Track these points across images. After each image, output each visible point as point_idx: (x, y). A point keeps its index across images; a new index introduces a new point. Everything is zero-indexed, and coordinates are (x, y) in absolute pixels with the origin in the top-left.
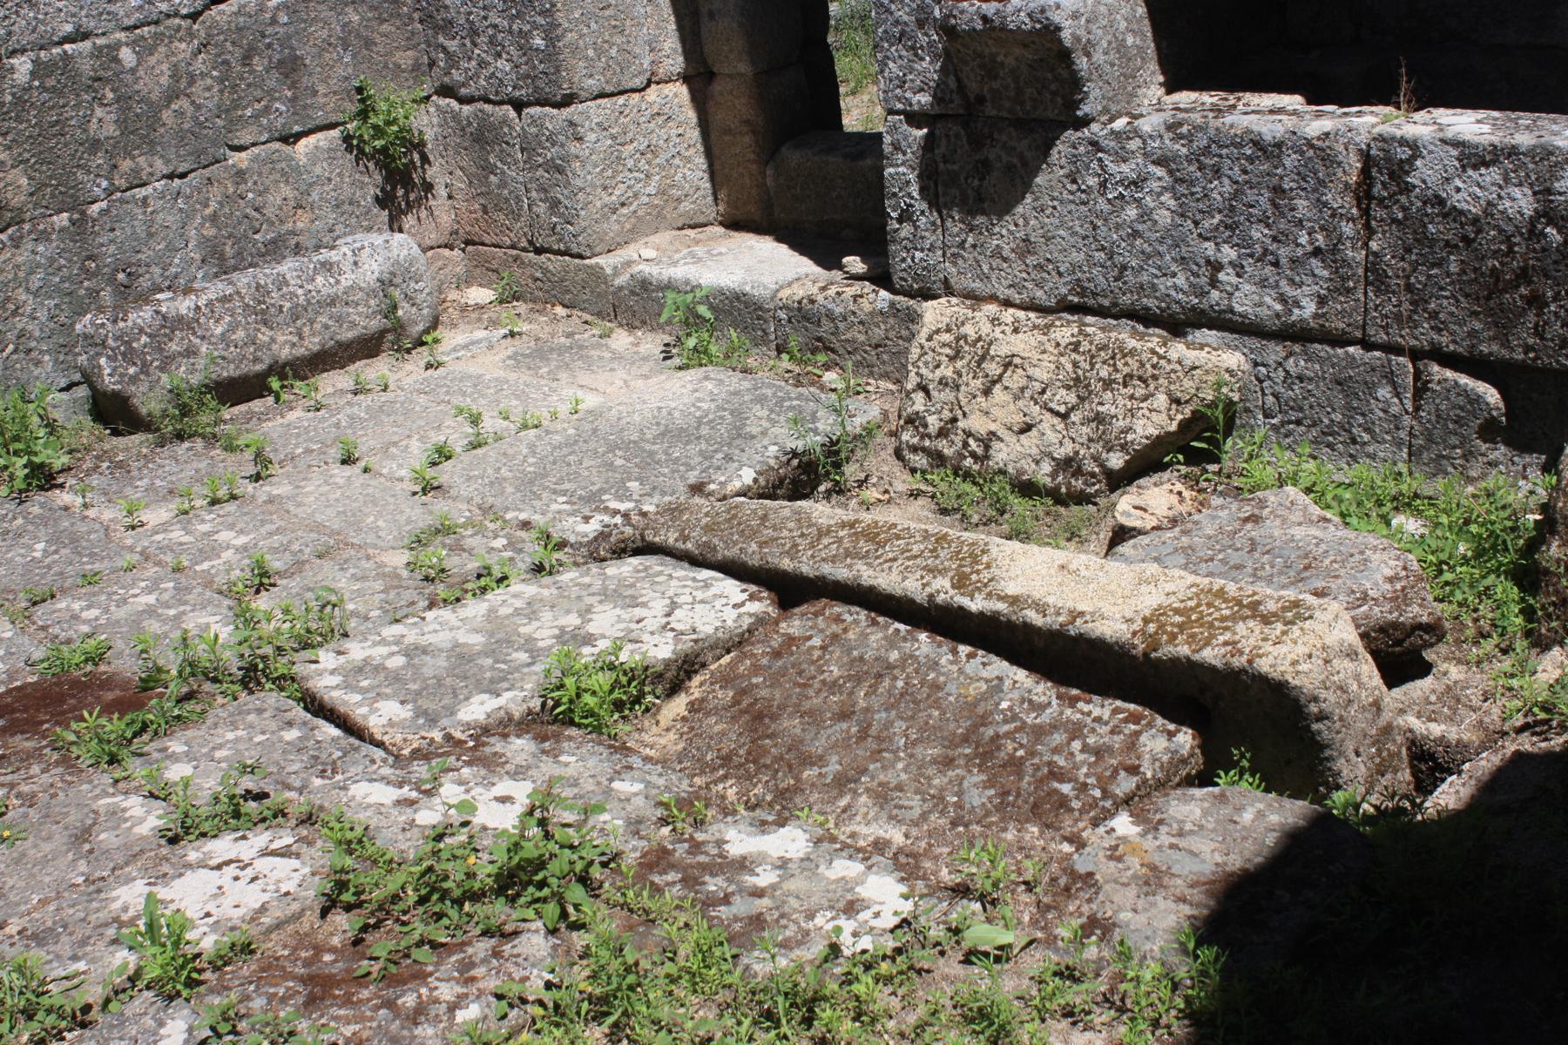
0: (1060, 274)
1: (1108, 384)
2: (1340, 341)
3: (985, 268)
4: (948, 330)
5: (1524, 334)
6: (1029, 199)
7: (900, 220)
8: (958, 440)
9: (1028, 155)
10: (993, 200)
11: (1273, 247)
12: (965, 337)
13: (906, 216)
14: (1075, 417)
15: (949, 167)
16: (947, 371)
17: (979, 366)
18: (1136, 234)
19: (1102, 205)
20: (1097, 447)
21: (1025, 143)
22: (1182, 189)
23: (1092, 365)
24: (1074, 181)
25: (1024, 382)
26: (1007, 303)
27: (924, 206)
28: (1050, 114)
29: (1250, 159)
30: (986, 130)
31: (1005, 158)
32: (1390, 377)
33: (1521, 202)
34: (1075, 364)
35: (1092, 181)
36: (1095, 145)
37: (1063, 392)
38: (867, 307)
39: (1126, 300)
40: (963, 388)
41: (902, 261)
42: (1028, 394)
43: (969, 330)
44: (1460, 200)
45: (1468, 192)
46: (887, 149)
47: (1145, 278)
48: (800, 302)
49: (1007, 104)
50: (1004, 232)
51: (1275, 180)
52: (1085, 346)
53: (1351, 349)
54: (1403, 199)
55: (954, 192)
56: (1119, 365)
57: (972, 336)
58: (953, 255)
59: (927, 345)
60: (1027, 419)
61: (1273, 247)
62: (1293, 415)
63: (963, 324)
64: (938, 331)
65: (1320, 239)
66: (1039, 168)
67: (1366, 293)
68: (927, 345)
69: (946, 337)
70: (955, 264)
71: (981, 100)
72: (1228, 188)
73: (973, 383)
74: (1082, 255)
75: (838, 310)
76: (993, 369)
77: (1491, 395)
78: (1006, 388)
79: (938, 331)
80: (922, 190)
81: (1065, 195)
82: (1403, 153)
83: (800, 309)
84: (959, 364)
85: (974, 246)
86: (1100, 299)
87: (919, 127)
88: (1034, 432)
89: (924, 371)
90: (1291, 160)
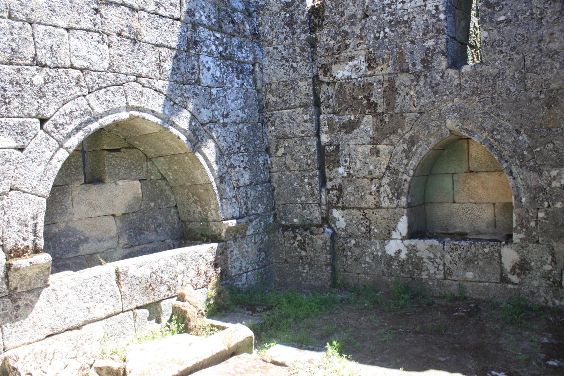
0: (46, 328)
1: (82, 344)
3: (20, 336)
4: (30, 354)
5: (152, 296)
6: (34, 311)
9: (33, 299)
10: (21, 316)
11: (102, 298)
14: (78, 356)
15: (4, 312)
16: (35, 365)
18: (67, 308)
19: (57, 304)
20: (87, 361)
21: (31, 296)
22: (78, 293)
24: (48, 301)
26: (29, 343)
28: (39, 286)
29: (94, 281)
30: (17, 297)
31: (25, 302)
32: (129, 317)
33: (149, 272)
36: (54, 290)
39: (66, 327)
44: (137, 275)
45: (139, 273)
47: (71, 319)
49: (25, 287)
50: (26, 323)
51: (100, 284)
52: (73, 339)
54: (127, 278)
55: (8, 318)
56: (83, 338)
57: (39, 352)
60: (66, 364)
61: (102, 298)
62: (111, 335)
64: (26, 356)
65: (112, 293)
71: (16, 288)
72: (90, 289)
74: (52, 320)
76: (50, 356)
77: (146, 311)
79: (26, 356)
81: (46, 306)
82: (126, 269)
84: (38, 361)
85: (15, 332)
86: (59, 330)
90: (103, 278)
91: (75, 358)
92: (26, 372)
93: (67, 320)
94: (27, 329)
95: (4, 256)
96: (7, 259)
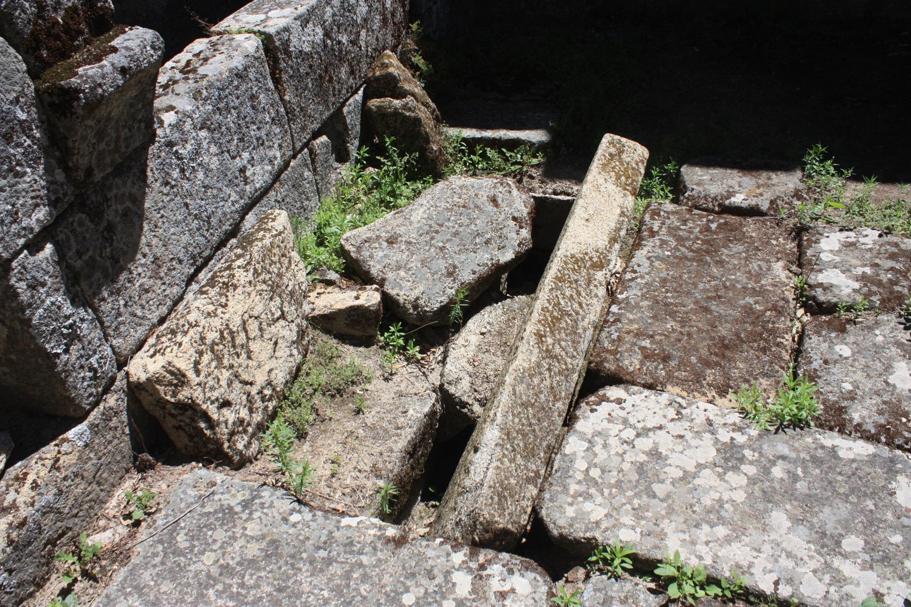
2: (286, 165)
3: (139, 313)
4: (201, 353)
7: (66, 351)
8: (259, 404)
12: (214, 343)
13: (73, 337)
15: (85, 258)
17: (234, 346)
23: (269, 272)
25: (257, 323)
27: (82, 311)
31: (120, 208)
34: (264, 282)
35: (176, 174)
37: (272, 303)
38: (71, 459)
40: (240, 370)
41: (81, 385)
42: (264, 326)
43: (212, 336)
46: (25, 297)
48: (11, 542)
50: (140, 270)
53: (292, 164)
58: (117, 328)
59: (202, 378)
63: (203, 339)
64: (197, 363)
66: (145, 193)
67: (290, 126)
68: (202, 378)
69: (206, 358)
70: (119, 335)
71: (89, 172)
73: (241, 360)
75: (50, 497)
78: (254, 339)
79: (197, 363)
80: (73, 303)
81: (166, 199)
83: (16, 549)
84: (226, 362)
85: (126, 305)
87: (42, 248)
88: (280, 341)
89: (216, 394)
91: (283, 316)
92: (216, 404)
93: (214, 221)
94: (148, 283)
95: (15, 62)
96: (34, 74)
